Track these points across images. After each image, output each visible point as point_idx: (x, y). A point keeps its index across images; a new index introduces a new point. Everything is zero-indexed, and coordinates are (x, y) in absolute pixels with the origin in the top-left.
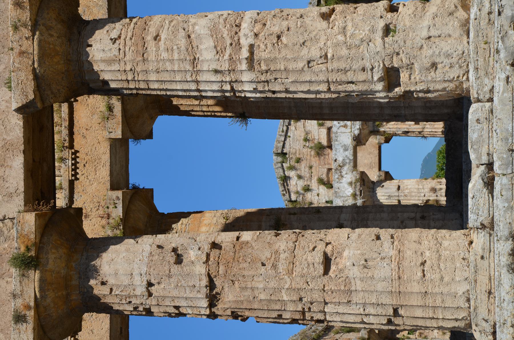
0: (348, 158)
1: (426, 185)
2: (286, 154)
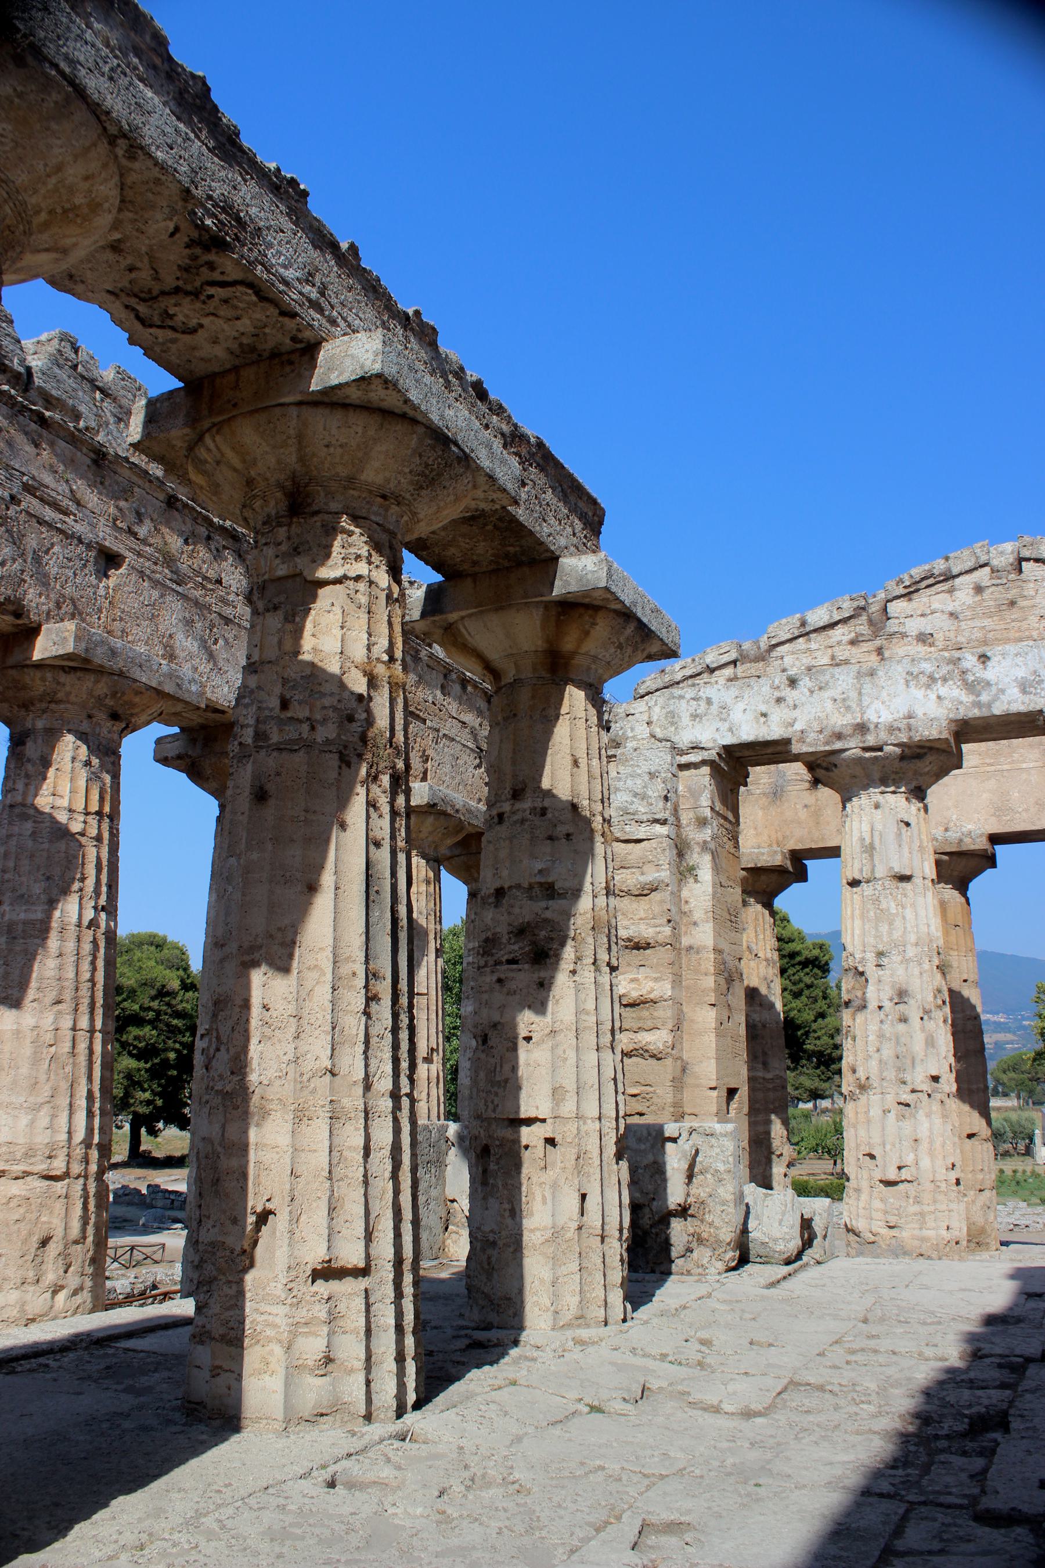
0: (996, 698)
2: (1020, 571)
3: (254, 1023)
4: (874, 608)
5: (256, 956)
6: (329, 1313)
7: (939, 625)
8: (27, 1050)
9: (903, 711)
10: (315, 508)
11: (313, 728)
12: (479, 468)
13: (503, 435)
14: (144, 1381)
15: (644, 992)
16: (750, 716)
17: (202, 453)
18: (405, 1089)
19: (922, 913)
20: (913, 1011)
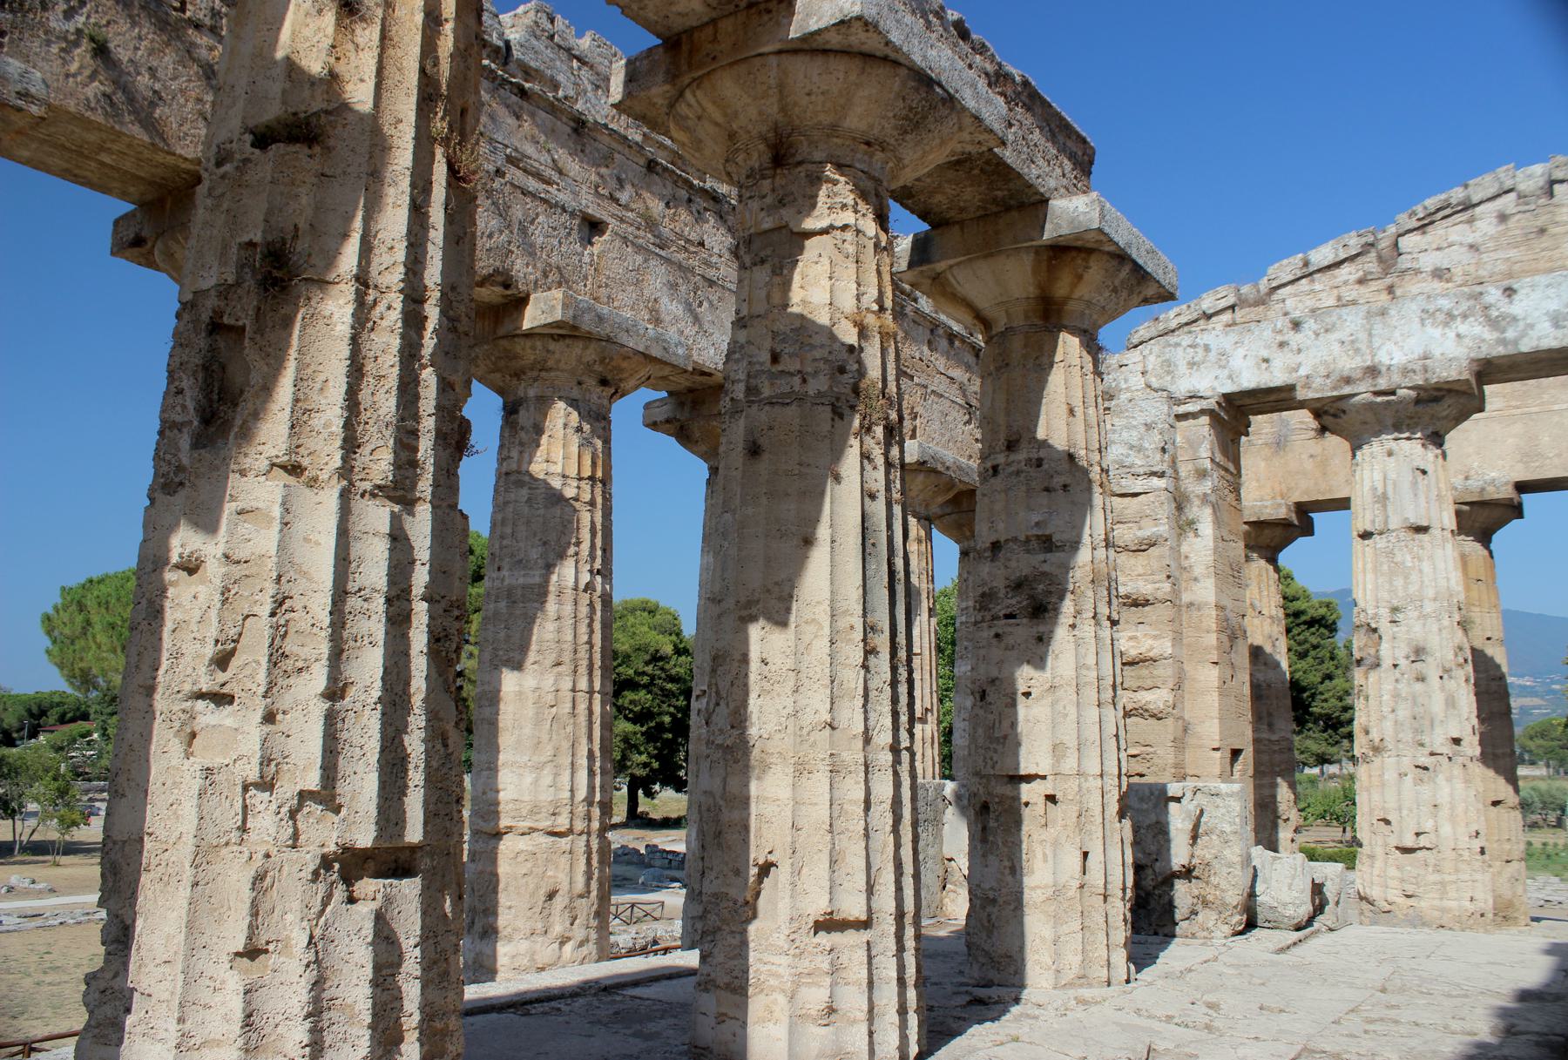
0: (1523, 335)
1: (1435, 628)
2: (1551, 194)
3: (753, 677)
4: (1384, 244)
5: (754, 611)
6: (832, 964)
7: (1457, 259)
8: (530, 711)
9: (1419, 351)
10: (799, 158)
11: (804, 381)
12: (964, 109)
13: (987, 74)
14: (652, 1027)
15: (1143, 650)
16: (1251, 362)
17: (682, 109)
18: (905, 743)
19: (1441, 565)
20: (1431, 669)
